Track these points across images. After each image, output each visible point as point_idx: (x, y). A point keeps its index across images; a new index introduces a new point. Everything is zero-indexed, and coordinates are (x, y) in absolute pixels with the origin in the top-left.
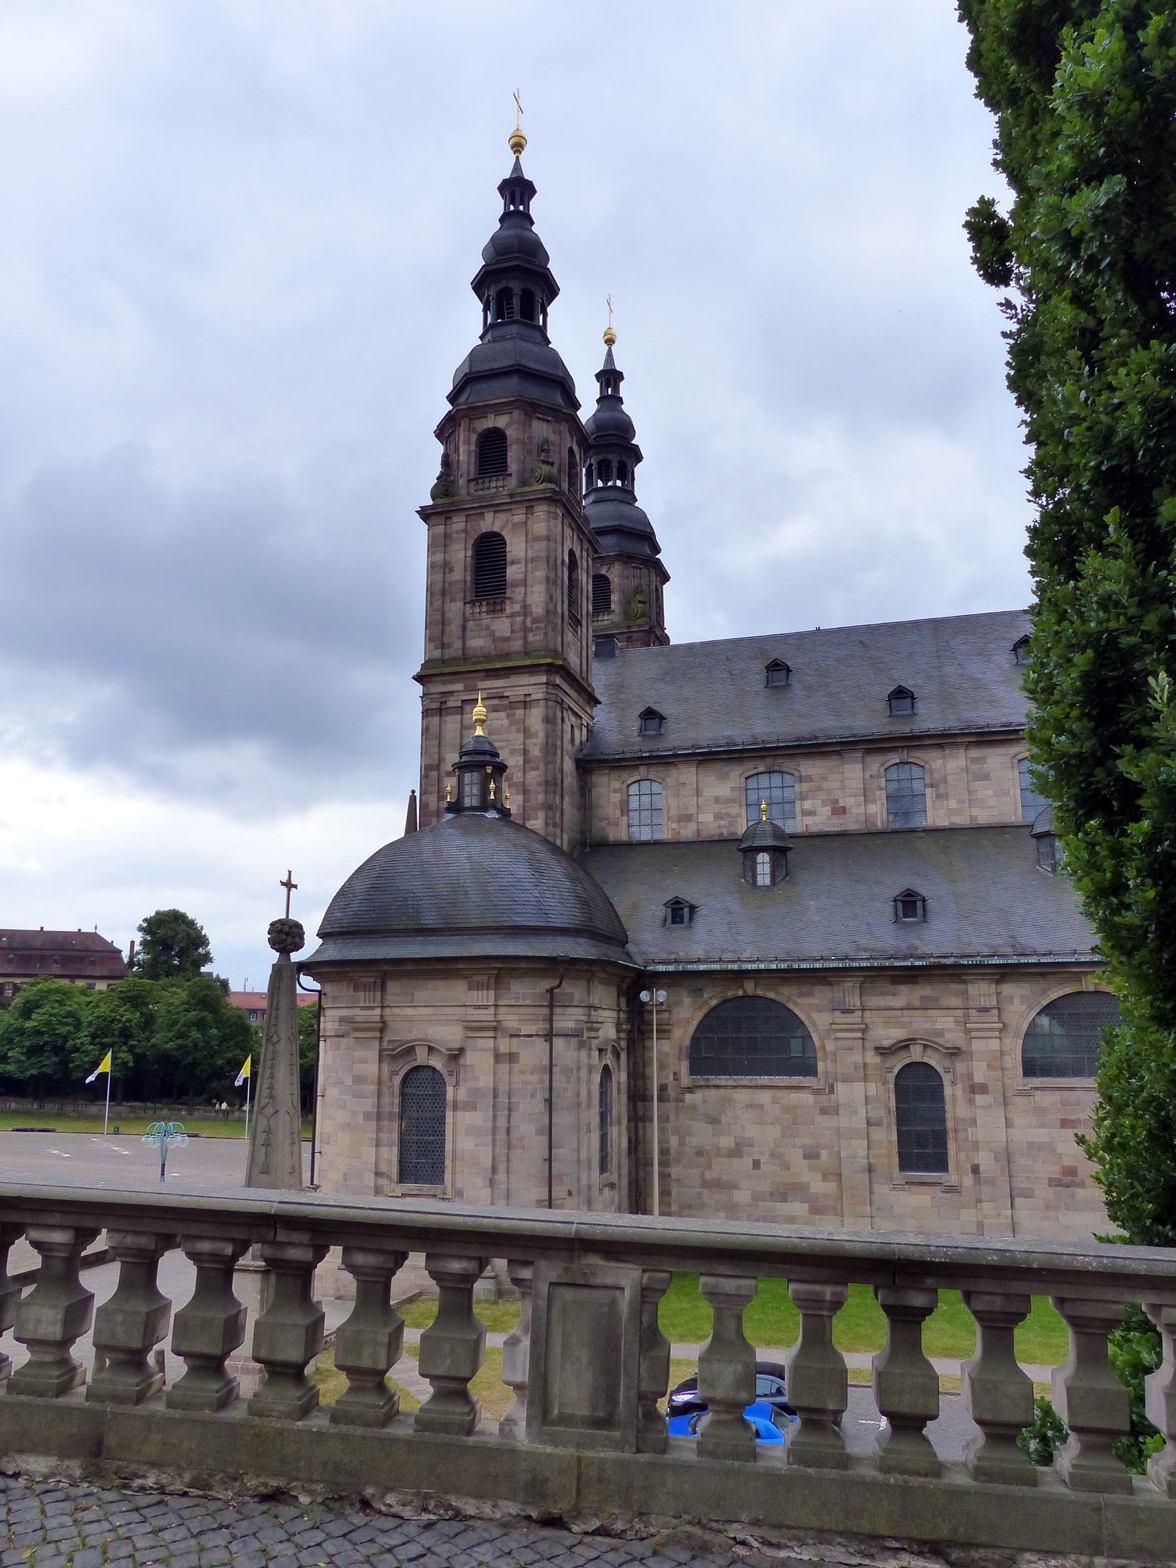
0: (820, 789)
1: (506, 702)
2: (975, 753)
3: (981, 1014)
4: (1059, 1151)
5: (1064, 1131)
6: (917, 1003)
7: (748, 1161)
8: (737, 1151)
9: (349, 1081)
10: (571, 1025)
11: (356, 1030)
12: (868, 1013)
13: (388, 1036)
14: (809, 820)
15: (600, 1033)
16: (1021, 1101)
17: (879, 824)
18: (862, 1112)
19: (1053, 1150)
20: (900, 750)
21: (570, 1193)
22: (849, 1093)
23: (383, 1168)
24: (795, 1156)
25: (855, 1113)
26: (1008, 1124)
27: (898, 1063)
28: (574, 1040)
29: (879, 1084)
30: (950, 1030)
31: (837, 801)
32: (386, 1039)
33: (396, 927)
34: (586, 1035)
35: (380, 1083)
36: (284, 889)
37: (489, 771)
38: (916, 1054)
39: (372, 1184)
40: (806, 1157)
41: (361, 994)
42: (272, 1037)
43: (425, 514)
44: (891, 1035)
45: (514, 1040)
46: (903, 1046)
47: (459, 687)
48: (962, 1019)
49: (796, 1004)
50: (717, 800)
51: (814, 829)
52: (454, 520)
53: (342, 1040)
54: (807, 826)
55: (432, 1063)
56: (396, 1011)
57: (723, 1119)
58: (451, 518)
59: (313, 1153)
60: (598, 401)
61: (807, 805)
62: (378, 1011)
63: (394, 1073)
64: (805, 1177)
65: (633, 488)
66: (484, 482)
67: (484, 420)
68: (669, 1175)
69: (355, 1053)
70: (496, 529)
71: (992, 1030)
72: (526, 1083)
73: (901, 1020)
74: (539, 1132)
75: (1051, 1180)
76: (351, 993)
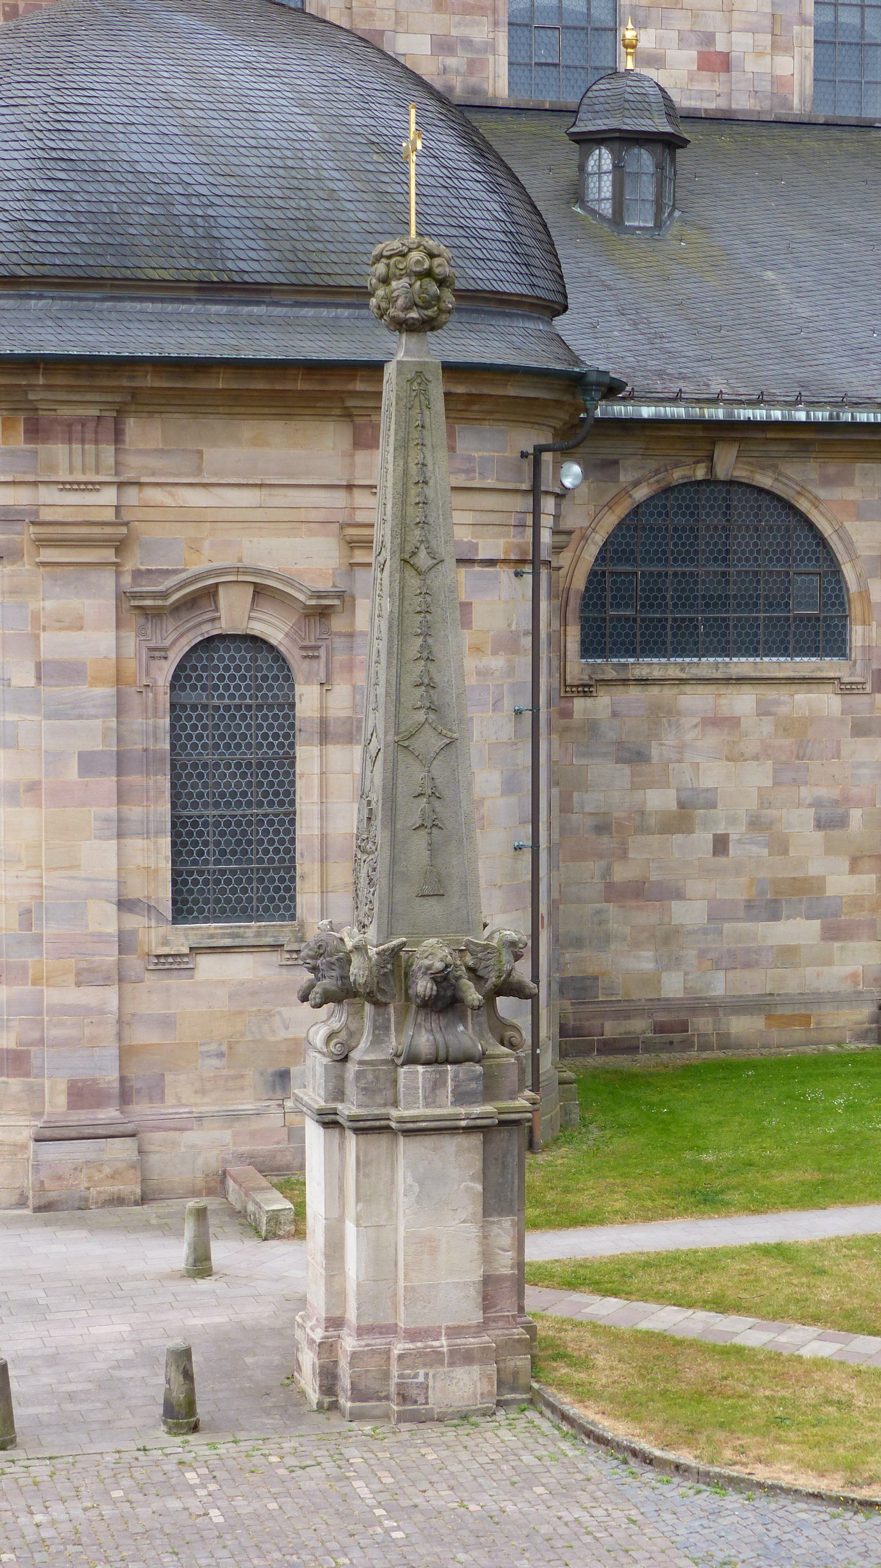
7: (703, 839)
11: (42, 543)
13: (134, 562)
23: (137, 890)
31: (709, 38)
32: (129, 567)
33: (154, 275)
35: (119, 679)
39: (112, 929)
40: (820, 825)
42: (414, 554)
49: (816, 502)
55: (258, 628)
57: (655, 752)
62: (109, 496)
63: (158, 653)
64: (814, 869)
69: (49, 604)
72: (483, 673)
74: (509, 787)
76: (19, 442)
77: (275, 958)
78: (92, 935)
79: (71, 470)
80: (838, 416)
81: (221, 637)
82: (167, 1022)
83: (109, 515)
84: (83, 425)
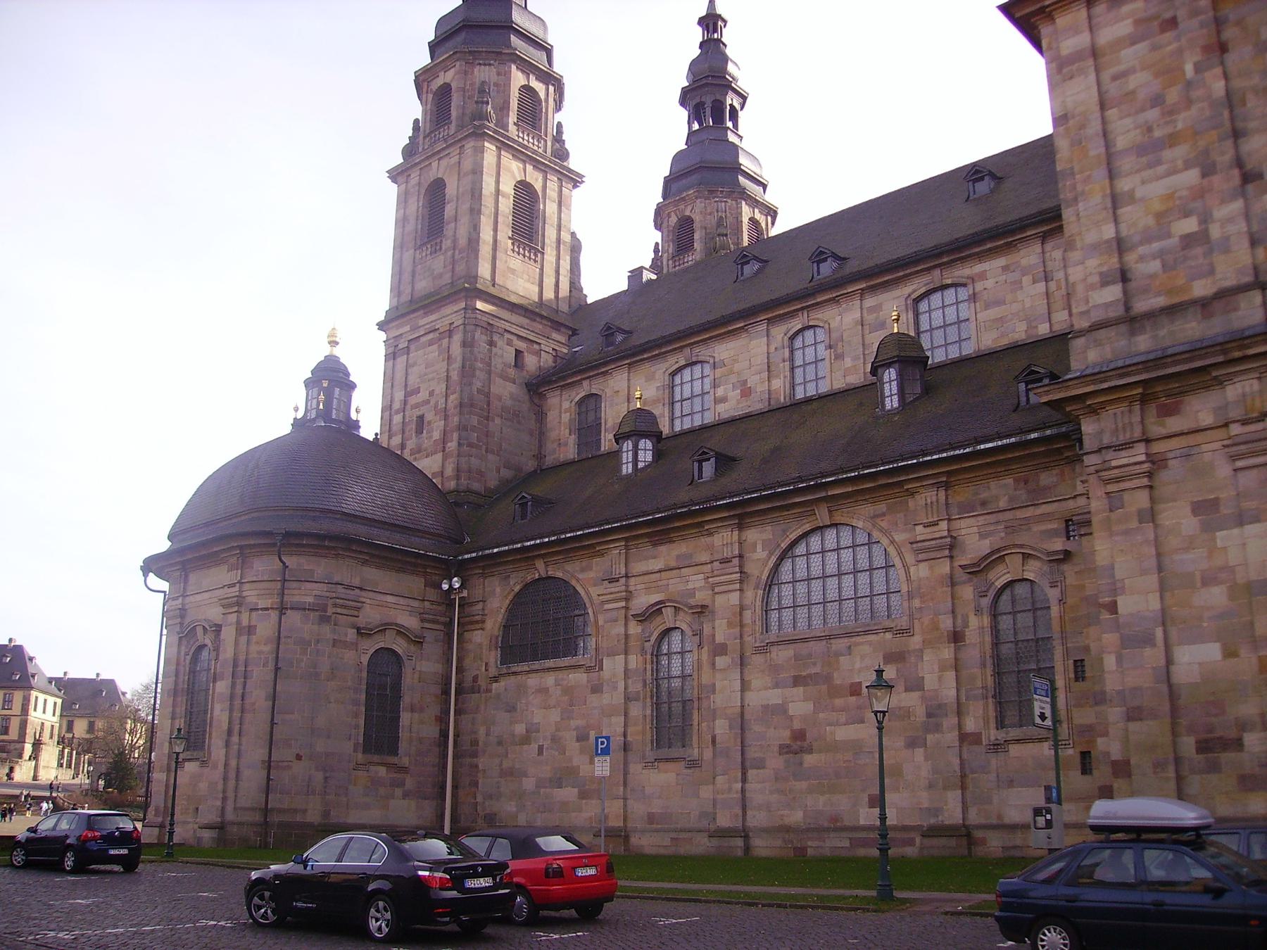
0: (732, 372)
2: (870, 302)
3: (723, 565)
4: (791, 713)
5: (795, 690)
6: (673, 564)
7: (535, 746)
8: (526, 740)
10: (310, 599)
14: (721, 408)
16: (758, 660)
19: (785, 711)
21: (299, 757)
22: (613, 666)
24: (569, 737)
25: (615, 688)
26: (745, 686)
30: (701, 589)
34: (330, 611)
40: (578, 740)
44: (643, 601)
45: (254, 614)
46: (655, 611)
47: (407, 328)
51: (725, 416)
61: (720, 392)
64: (576, 762)
66: (435, 135)
68: (477, 766)
70: (440, 176)
71: (731, 582)
72: (260, 652)
73: (660, 583)
75: (781, 746)
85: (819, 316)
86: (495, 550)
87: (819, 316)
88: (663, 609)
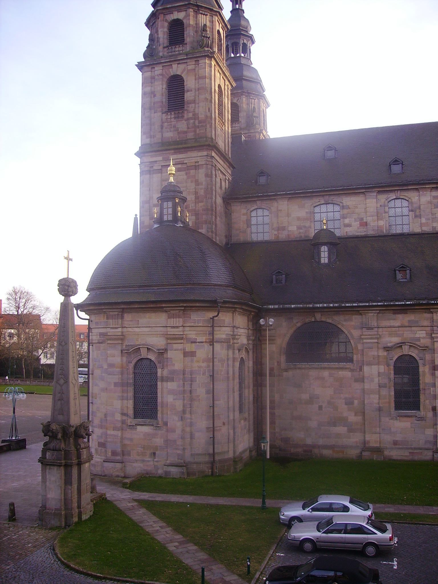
0: (354, 213)
1: (185, 166)
9: (105, 367)
10: (224, 336)
12: (380, 330)
13: (126, 343)
14: (348, 229)
15: (239, 341)
17: (385, 231)
18: (376, 380)
20: (396, 192)
21: (224, 424)
27: (396, 355)
28: (225, 345)
29: (385, 366)
30: (423, 338)
31: (362, 219)
34: (231, 342)
36: (66, 261)
37: (177, 201)
38: (406, 350)
39: (119, 419)
40: (346, 404)
41: (111, 321)
43: (140, 66)
45: (194, 344)
47: (160, 158)
48: (430, 332)
49: (343, 325)
50: (299, 219)
52: (156, 69)
53: (101, 345)
54: (346, 232)
56: (130, 329)
58: (154, 68)
59: (88, 403)
60: (231, 12)
62: (120, 330)
64: (345, 414)
65: (250, 57)
67: (172, 15)
68: (275, 414)
70: (179, 73)
72: (200, 367)
73: (398, 332)
74: (207, 392)
77: (152, 427)
78: (116, 420)
79: (113, 325)
80: (341, 305)
81: (142, 359)
82: (131, 440)
83: (120, 334)
84: (115, 316)
85: (406, 195)
86: (293, 306)
87: (406, 195)
88: (403, 346)
